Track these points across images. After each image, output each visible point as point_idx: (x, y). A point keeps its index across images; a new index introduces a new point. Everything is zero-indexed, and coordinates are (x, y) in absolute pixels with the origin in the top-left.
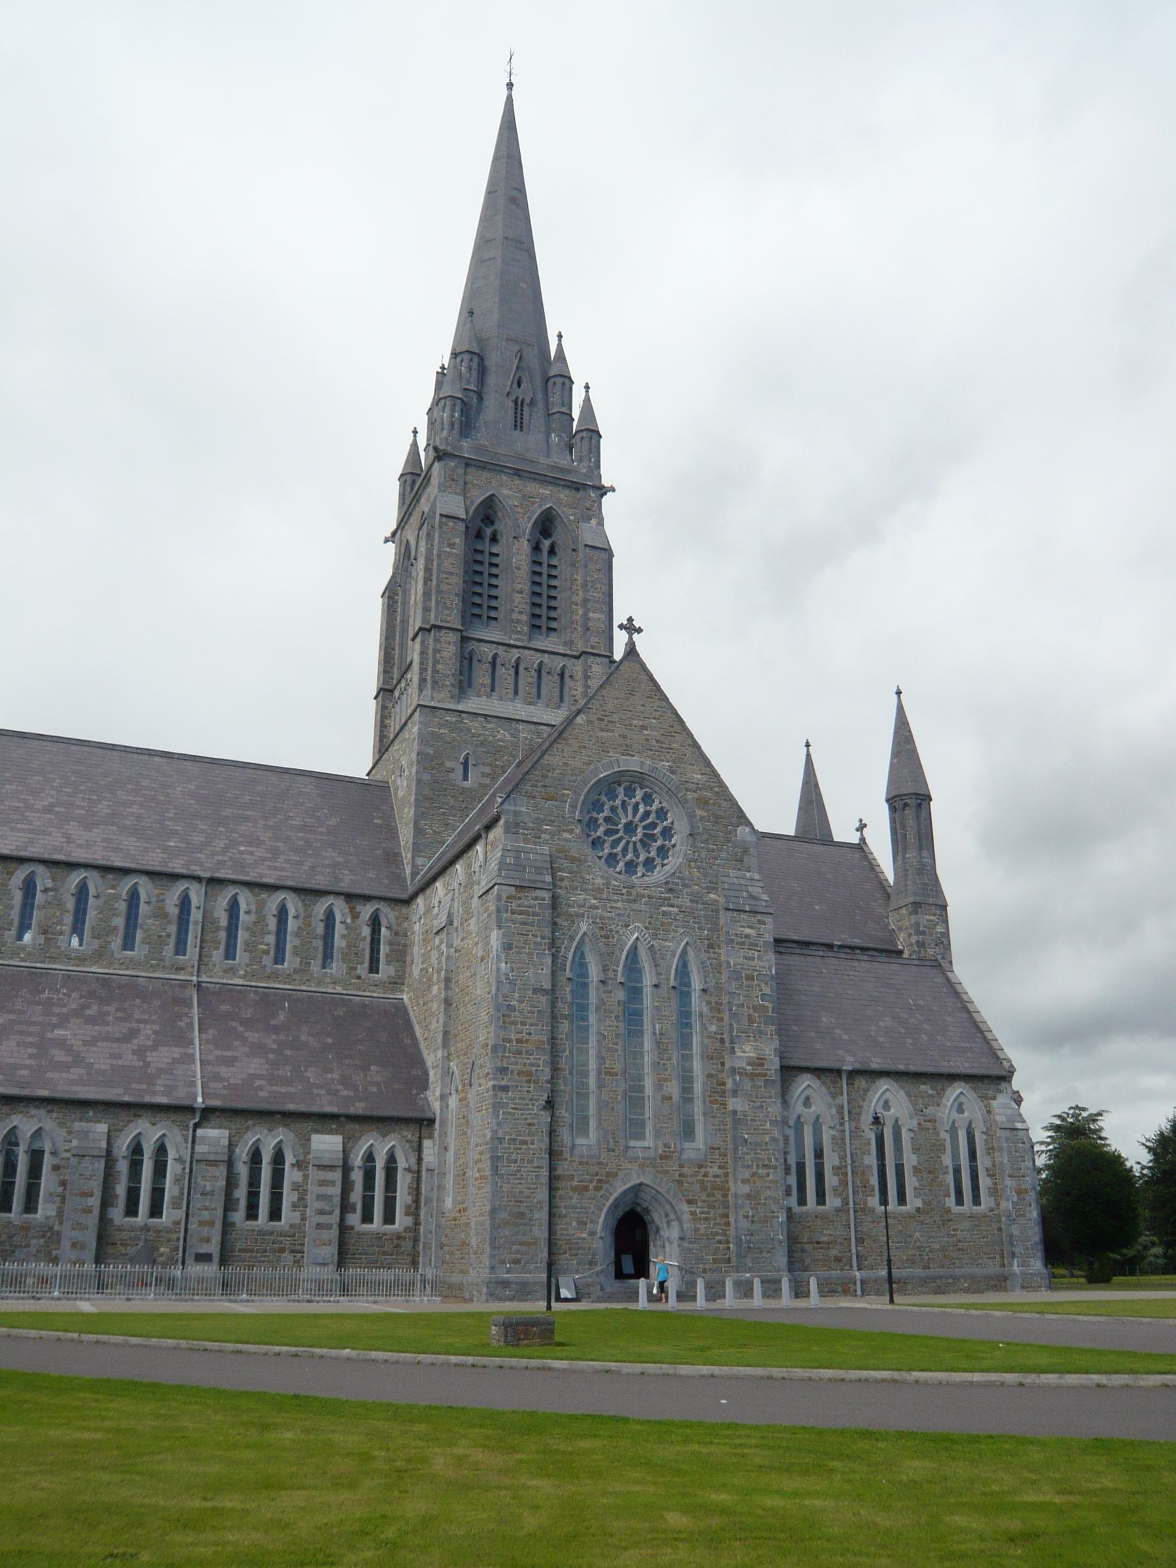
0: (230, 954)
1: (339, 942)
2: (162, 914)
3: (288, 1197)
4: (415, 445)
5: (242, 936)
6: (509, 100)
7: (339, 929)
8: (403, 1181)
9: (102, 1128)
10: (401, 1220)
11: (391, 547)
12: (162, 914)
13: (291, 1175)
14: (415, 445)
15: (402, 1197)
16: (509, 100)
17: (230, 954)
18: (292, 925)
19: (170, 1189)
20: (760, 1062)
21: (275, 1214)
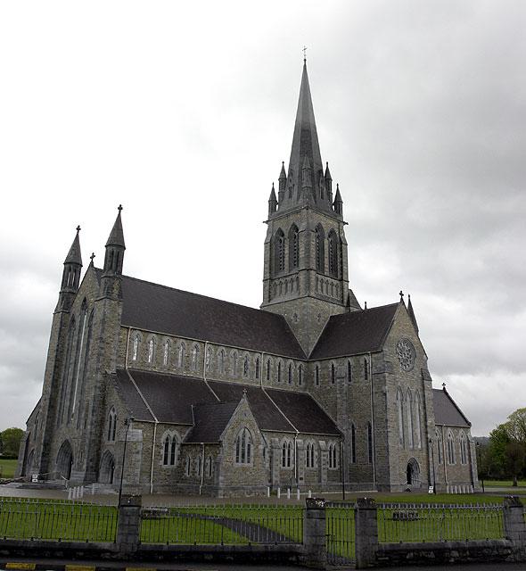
0: (268, 379)
1: (293, 375)
2: (252, 365)
3: (315, 460)
4: (273, 189)
5: (271, 372)
6: (305, 65)
7: (293, 370)
8: (337, 454)
9: (277, 439)
10: (338, 467)
11: (266, 226)
12: (252, 365)
13: (316, 453)
14: (273, 189)
15: (337, 460)
16: (305, 65)
17: (268, 379)
18: (282, 368)
19: (292, 458)
20: (431, 424)
21: (312, 466)
